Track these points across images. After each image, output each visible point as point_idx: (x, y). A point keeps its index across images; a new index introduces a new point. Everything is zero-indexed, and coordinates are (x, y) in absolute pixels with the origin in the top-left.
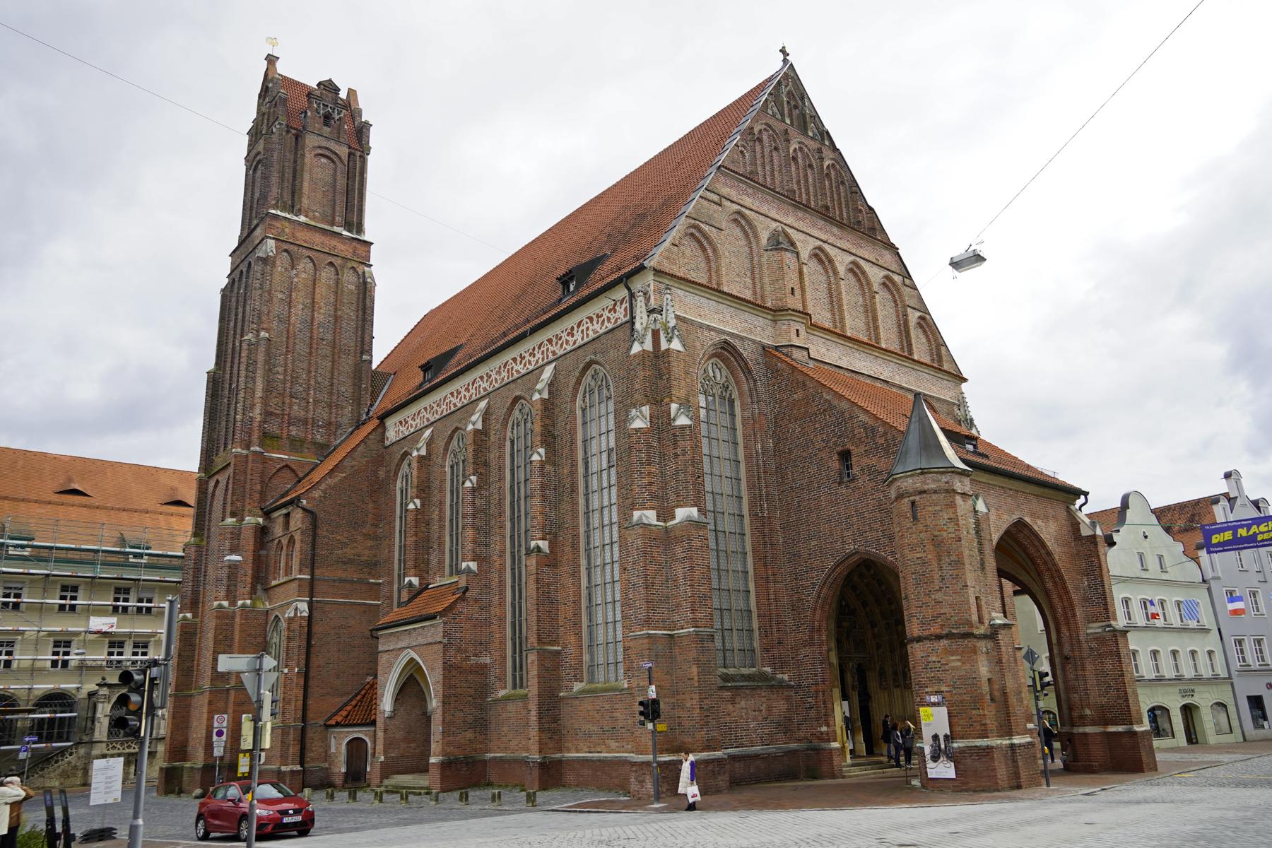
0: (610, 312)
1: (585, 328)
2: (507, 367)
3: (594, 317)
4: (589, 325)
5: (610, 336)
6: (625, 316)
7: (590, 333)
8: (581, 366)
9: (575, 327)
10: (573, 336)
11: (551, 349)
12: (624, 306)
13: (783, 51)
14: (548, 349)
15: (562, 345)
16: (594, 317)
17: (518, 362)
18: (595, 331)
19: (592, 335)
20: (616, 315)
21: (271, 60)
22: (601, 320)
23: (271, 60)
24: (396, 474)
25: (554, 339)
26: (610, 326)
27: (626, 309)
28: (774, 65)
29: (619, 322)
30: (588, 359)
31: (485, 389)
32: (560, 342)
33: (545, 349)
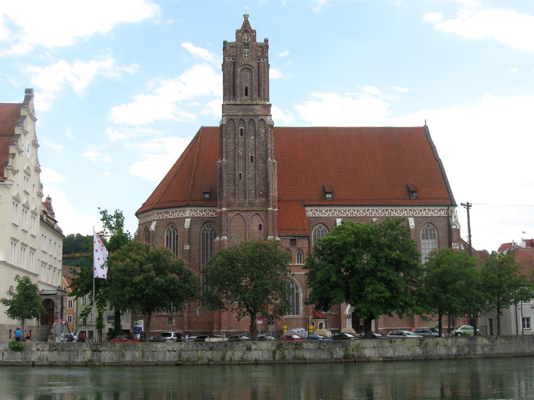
0: (438, 211)
1: (427, 212)
2: (388, 211)
3: (431, 210)
4: (429, 211)
5: (438, 218)
6: (444, 214)
7: (429, 214)
8: (426, 222)
9: (423, 210)
10: (422, 212)
11: (411, 213)
12: (444, 211)
13: (425, 122)
14: (409, 213)
15: (416, 213)
16: (431, 210)
17: (394, 212)
18: (431, 214)
19: (430, 215)
20: (441, 213)
21: (246, 17)
22: (434, 212)
23: (246, 17)
24: (313, 229)
25: (412, 210)
26: (438, 215)
27: (444, 213)
28: (422, 125)
29: (442, 215)
30: (428, 221)
31: (375, 214)
32: (415, 212)
33: (408, 212)
